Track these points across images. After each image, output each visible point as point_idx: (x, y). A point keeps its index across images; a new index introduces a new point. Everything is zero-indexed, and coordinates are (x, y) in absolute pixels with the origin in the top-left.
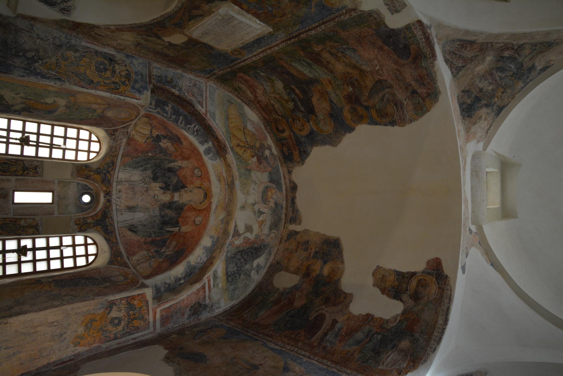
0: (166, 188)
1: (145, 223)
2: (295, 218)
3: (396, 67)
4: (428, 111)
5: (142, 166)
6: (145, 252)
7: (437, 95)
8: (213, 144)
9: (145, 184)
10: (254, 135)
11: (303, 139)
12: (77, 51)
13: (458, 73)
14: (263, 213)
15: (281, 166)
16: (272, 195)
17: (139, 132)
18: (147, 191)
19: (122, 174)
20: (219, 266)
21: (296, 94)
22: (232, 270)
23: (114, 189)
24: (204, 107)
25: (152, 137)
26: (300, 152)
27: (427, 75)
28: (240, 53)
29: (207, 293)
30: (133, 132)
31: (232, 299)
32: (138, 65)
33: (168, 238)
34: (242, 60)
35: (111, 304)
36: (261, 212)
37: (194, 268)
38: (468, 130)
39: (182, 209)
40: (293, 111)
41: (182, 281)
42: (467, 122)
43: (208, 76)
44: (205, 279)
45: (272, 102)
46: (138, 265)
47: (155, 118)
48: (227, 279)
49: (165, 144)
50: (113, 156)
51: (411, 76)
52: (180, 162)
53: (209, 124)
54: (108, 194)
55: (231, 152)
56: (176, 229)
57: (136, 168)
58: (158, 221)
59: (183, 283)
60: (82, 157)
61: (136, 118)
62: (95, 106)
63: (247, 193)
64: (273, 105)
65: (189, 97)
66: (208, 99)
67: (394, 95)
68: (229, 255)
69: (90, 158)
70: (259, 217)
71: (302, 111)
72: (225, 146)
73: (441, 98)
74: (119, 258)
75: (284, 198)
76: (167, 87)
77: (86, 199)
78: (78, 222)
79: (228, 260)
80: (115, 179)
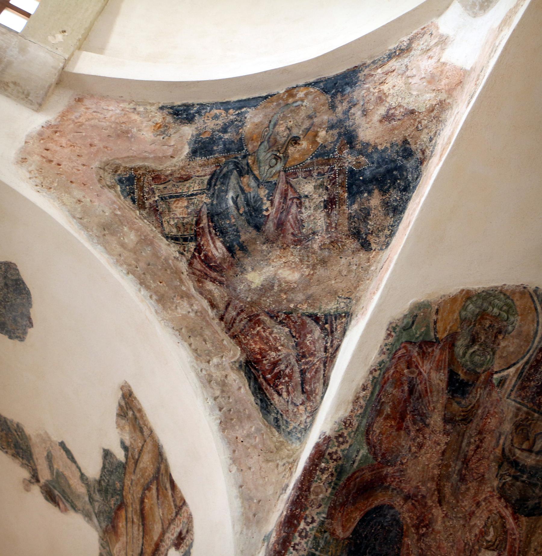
3: (438, 512)
4: (468, 296)
7: (406, 328)
13: (338, 316)
27: (379, 413)
38: (438, 111)
42: (424, 137)
51: (421, 446)
67: (522, 428)
73: (400, 309)
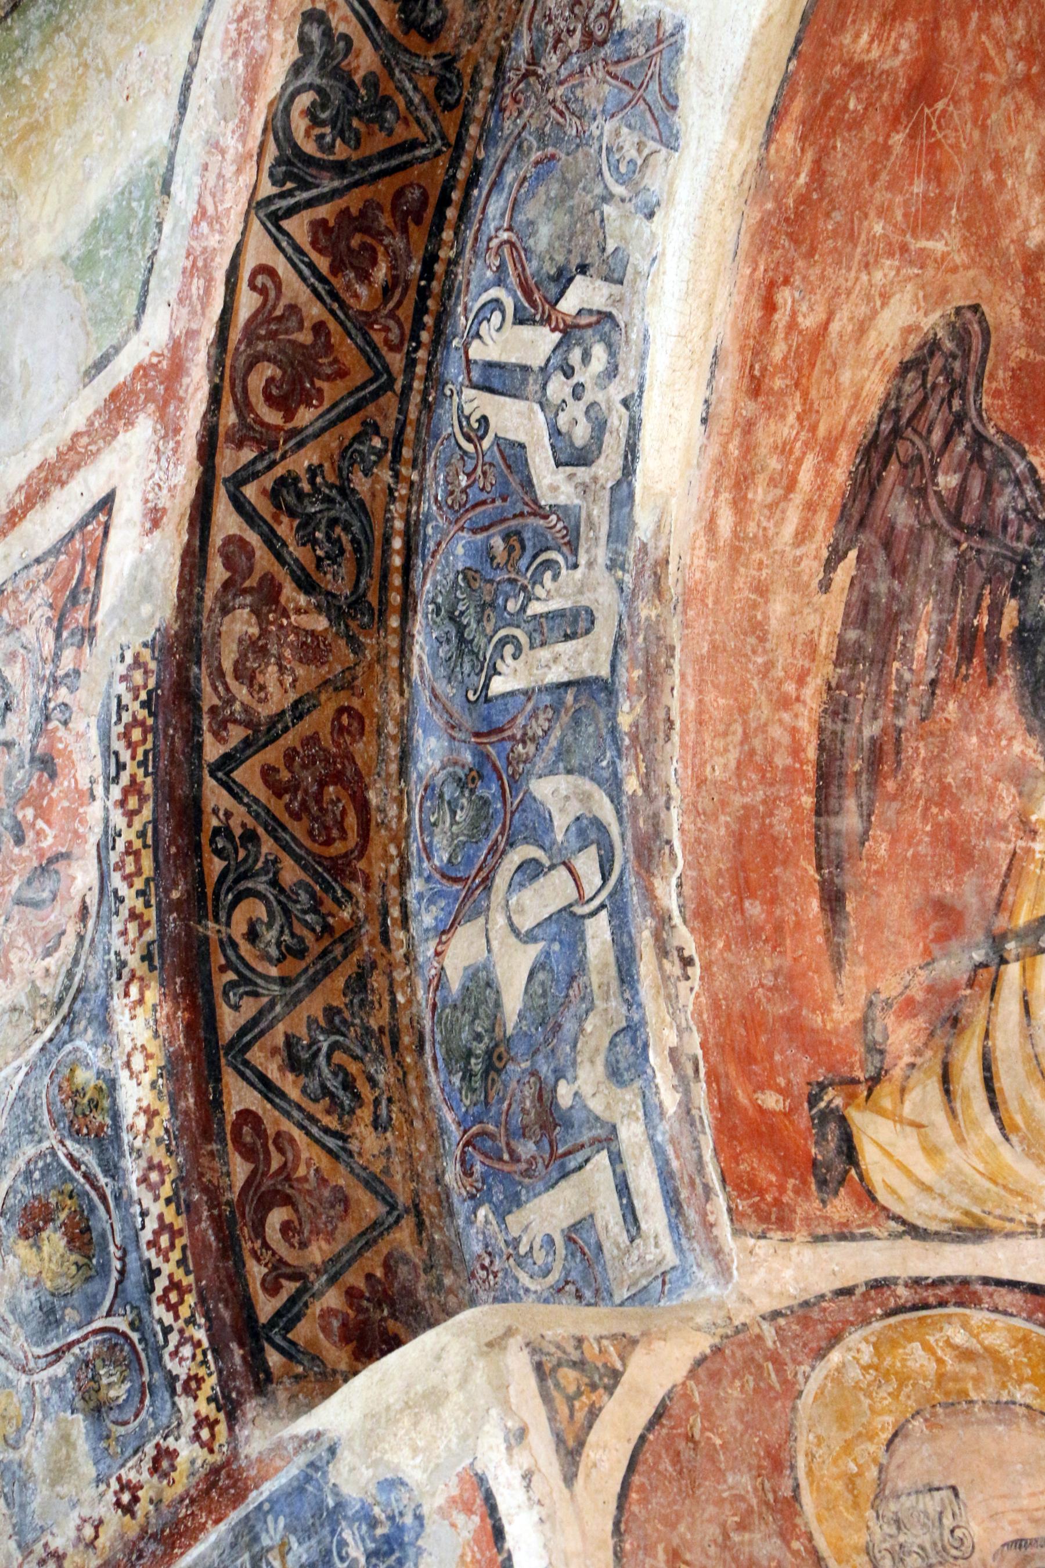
53: (270, 214)
61: (962, 1291)
76: (154, 1208)
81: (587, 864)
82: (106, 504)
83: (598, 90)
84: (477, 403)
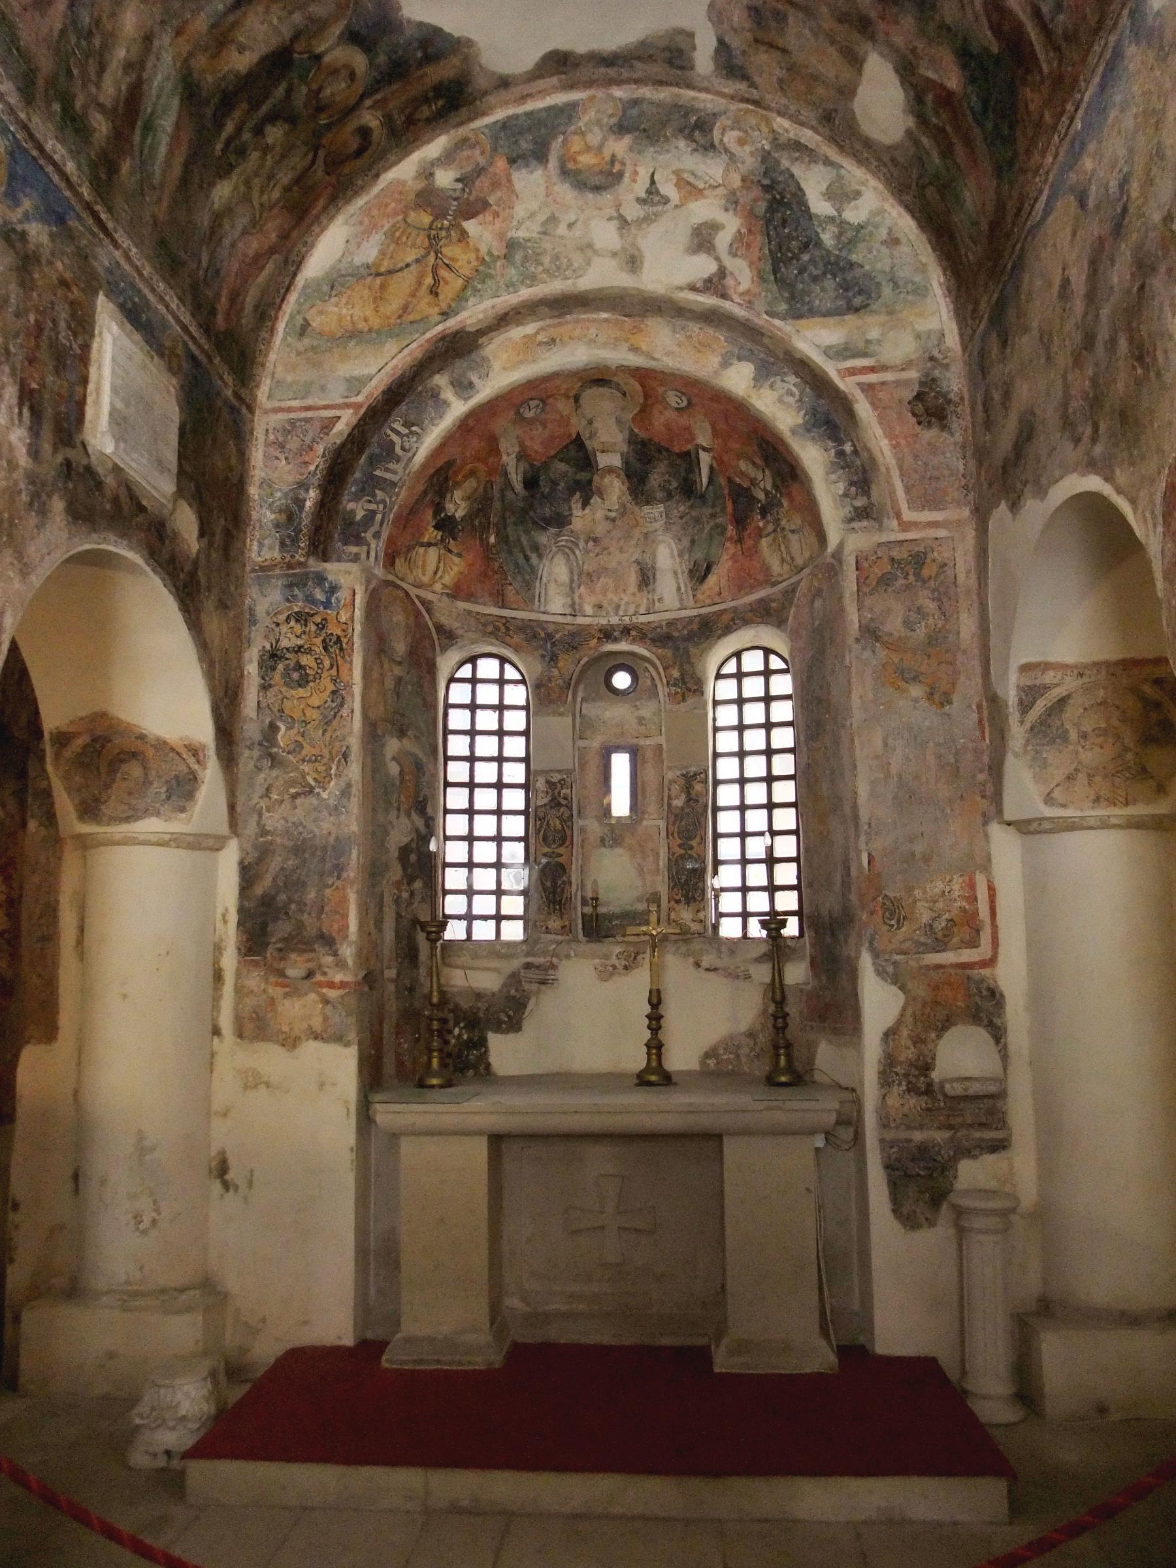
0: (586, 491)
1: (686, 542)
2: (669, 56)
5: (527, 558)
6: (764, 542)
8: (440, 370)
9: (577, 545)
10: (393, 237)
11: (382, 59)
12: (273, 728)
14: (653, 182)
15: (484, 114)
16: (588, 149)
17: (435, 573)
18: (595, 540)
19: (554, 605)
20: (814, 339)
21: (239, 129)
22: (832, 294)
23: (595, 621)
24: (337, 413)
25: (442, 540)
26: (429, 59)
28: (172, 350)
29: (889, 376)
30: (438, 587)
31: (921, 291)
32: (266, 601)
33: (730, 480)
34: (186, 338)
35: (871, 633)
36: (649, 192)
37: (813, 412)
39: (644, 443)
40: (292, 120)
41: (848, 448)
43: (244, 410)
44: (845, 385)
45: (276, 194)
46: (792, 559)
47: (391, 541)
48: (857, 310)
49: (457, 506)
50: (508, 629)
52: (504, 457)
53: (384, 392)
54: (607, 634)
55: (459, 318)
56: (705, 458)
57: (533, 571)
58: (682, 508)
59: (854, 446)
60: (516, 695)
62: (389, 683)
63: (587, 248)
64: (287, 189)
65: (317, 461)
66: (309, 402)
68: (783, 307)
69: (519, 677)
70: (666, 201)
71: (289, 91)
72: (443, 338)
74: (773, 605)
75: (600, 93)
77: (622, 680)
78: (679, 697)
79: (799, 308)
80: (569, 619)
81: (381, 507)
82: (339, 418)
83: (430, 402)
84: (389, 432)
